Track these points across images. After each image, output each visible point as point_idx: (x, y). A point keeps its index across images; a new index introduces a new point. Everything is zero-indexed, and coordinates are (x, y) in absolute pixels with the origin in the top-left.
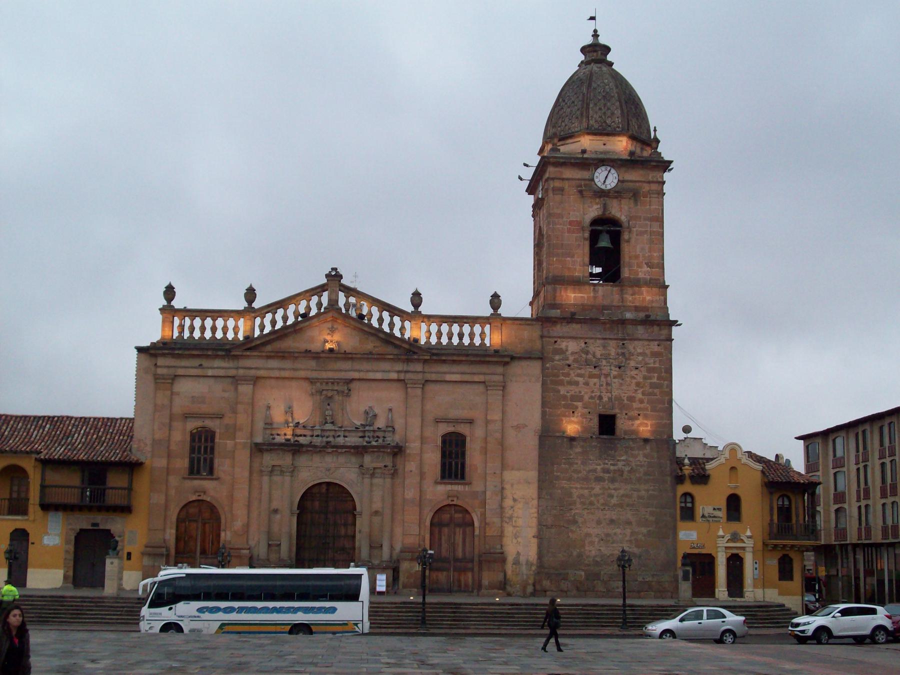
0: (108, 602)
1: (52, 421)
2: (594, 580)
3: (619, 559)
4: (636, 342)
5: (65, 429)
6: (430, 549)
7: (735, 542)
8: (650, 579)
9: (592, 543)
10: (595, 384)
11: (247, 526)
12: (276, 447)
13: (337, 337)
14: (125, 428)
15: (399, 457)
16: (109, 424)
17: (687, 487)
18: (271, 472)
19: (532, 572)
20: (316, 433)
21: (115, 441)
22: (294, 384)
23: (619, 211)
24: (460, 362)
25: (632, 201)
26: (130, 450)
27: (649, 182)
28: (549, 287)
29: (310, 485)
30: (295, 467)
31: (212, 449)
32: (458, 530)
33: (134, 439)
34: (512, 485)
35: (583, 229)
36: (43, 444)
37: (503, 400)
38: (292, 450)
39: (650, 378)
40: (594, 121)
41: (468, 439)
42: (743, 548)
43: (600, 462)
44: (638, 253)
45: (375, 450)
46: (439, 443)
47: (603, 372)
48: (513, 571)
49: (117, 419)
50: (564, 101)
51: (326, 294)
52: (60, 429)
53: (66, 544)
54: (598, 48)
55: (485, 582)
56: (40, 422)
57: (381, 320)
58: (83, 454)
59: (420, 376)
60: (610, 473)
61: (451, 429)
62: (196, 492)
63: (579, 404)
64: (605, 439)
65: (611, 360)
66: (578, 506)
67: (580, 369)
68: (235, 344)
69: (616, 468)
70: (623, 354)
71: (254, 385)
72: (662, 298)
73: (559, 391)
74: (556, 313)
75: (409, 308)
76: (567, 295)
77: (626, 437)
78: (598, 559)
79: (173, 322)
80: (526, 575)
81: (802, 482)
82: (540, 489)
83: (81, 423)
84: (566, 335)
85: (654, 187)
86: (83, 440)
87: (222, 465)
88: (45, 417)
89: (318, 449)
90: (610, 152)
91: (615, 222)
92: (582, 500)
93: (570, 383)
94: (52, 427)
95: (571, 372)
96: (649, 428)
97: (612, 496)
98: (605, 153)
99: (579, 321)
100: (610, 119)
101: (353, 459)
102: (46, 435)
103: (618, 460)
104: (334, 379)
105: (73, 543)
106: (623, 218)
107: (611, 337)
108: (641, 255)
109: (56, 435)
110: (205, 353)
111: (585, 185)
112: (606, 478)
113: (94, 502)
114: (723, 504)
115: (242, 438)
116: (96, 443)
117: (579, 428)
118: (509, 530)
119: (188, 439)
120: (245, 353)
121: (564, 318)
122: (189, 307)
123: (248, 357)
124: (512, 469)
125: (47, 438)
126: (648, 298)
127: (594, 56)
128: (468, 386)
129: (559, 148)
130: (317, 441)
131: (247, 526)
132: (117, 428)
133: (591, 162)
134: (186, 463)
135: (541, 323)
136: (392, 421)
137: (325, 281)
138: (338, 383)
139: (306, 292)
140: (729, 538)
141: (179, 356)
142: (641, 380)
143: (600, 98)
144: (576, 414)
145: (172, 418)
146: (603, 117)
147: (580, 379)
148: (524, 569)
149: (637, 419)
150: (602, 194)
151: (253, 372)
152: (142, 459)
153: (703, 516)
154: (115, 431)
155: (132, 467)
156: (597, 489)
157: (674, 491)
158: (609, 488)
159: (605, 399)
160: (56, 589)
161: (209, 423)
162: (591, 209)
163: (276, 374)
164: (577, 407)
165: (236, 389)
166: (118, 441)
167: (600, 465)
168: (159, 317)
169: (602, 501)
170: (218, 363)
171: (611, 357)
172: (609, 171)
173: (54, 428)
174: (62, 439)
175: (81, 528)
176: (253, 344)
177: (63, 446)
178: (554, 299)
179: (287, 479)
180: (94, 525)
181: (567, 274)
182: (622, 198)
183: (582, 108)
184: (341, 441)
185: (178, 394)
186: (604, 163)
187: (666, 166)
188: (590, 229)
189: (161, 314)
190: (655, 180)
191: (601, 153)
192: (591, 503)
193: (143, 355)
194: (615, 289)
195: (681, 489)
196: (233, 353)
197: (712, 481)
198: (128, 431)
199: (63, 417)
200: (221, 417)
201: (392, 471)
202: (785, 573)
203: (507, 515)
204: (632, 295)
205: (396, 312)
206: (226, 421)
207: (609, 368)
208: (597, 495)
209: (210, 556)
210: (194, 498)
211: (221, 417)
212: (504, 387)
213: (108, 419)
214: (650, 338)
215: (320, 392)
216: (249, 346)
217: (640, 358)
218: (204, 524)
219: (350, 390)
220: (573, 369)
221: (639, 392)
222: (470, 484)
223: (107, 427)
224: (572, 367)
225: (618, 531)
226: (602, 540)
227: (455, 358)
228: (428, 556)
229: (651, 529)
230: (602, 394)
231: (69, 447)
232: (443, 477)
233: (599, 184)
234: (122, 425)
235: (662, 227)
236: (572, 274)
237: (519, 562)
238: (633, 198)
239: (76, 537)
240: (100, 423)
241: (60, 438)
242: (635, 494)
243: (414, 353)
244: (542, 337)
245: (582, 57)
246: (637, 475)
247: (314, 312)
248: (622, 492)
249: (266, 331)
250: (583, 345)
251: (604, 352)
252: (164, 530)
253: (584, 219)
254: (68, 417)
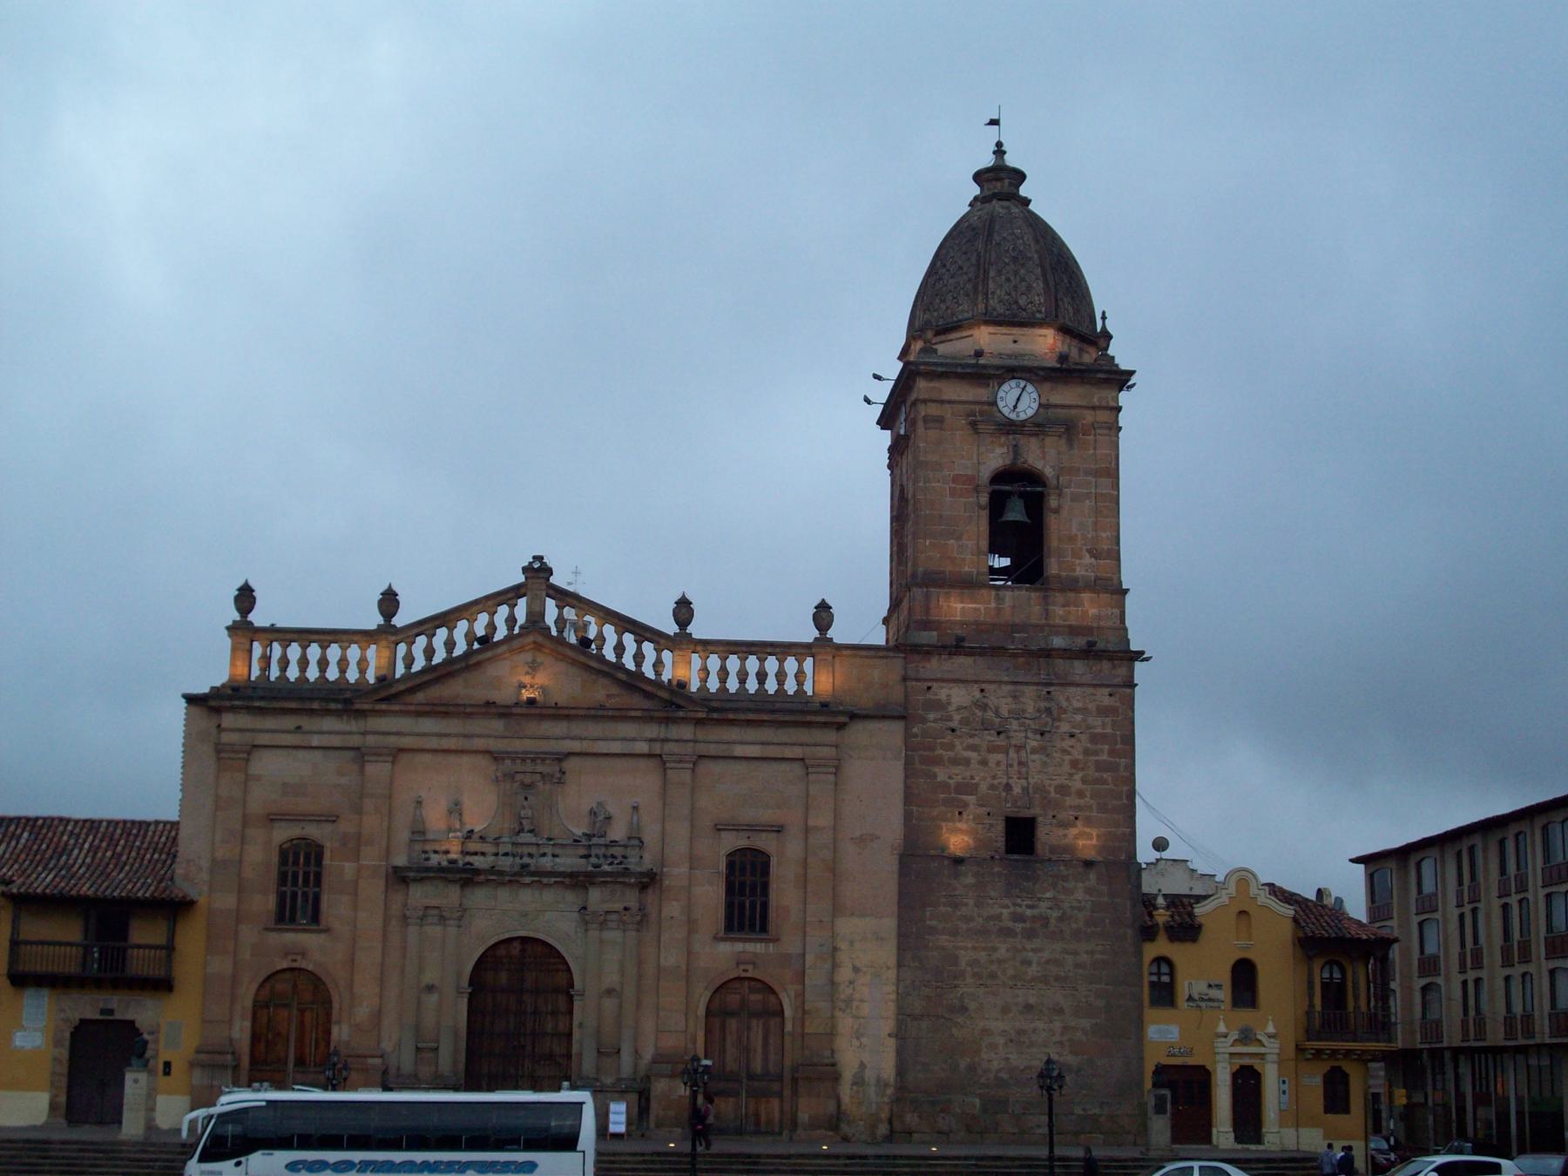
0: (129, 1152)
1: (33, 826)
2: (997, 1113)
3: (1041, 1075)
4: (1072, 690)
5: (55, 839)
6: (706, 1058)
7: (1246, 1045)
8: (1097, 1111)
9: (993, 1047)
10: (998, 764)
11: (378, 1015)
12: (431, 875)
13: (541, 678)
14: (163, 839)
15: (650, 891)
16: (135, 831)
17: (1161, 946)
18: (422, 920)
19: (886, 1099)
20: (502, 850)
21: (146, 862)
22: (466, 760)
23: (1041, 457)
24: (760, 723)
25: (1063, 441)
26: (172, 879)
27: (1094, 408)
28: (918, 592)
29: (492, 942)
30: (465, 910)
31: (318, 877)
32: (754, 1022)
33: (178, 860)
34: (852, 943)
35: (977, 489)
36: (16, 866)
37: (836, 790)
38: (461, 879)
39: (1096, 753)
40: (996, 301)
41: (774, 861)
42: (1262, 1056)
43: (1006, 901)
44: (1074, 531)
45: (609, 879)
46: (723, 866)
47: (1013, 742)
48: (852, 1097)
49: (148, 824)
50: (945, 266)
51: (522, 603)
52: (47, 841)
53: (55, 1047)
54: (1003, 175)
55: (803, 1117)
56: (12, 828)
57: (620, 649)
58: (87, 885)
59: (689, 748)
60: (1024, 921)
61: (742, 842)
62: (286, 954)
63: (971, 799)
64: (1016, 860)
65: (1027, 721)
66: (969, 980)
67: (972, 736)
68: (361, 690)
69: (1035, 912)
70: (1048, 711)
71: (393, 763)
72: (1117, 611)
73: (935, 776)
74: (930, 637)
75: (671, 628)
76: (949, 606)
77: (1054, 858)
78: (1005, 1076)
79: (250, 651)
80: (877, 1103)
81: (1365, 937)
82: (902, 948)
83: (85, 830)
84: (947, 676)
85: (1103, 416)
86: (88, 860)
87: (334, 906)
88: (19, 819)
89: (507, 878)
90: (1024, 355)
91: (1032, 478)
92: (975, 970)
93: (955, 761)
94: (33, 837)
95: (957, 742)
96: (1094, 842)
97: (1027, 963)
98: (1016, 356)
99: (971, 652)
100: (1024, 297)
101: (570, 896)
102: (22, 851)
103: (1040, 899)
104: (536, 753)
105: (67, 1043)
106: (1049, 472)
107: (1027, 679)
108: (1080, 537)
109: (41, 852)
110: (307, 705)
111: (982, 413)
112: (1018, 930)
113: (106, 971)
114: (1225, 978)
115: (371, 857)
116: (111, 866)
117: (971, 841)
118: (845, 1024)
119: (275, 859)
120: (378, 707)
121: (944, 647)
122: (280, 624)
123: (383, 713)
124: (852, 914)
125: (23, 856)
126: (1093, 611)
127: (998, 187)
128: (775, 766)
129: (935, 347)
130: (505, 863)
131: (378, 1016)
132: (148, 839)
133: (992, 372)
134: (271, 902)
135: (903, 655)
136: (639, 828)
137: (521, 579)
138: (543, 760)
139: (488, 598)
140: (1236, 1037)
141: (261, 711)
142: (1081, 757)
143: (1007, 260)
144: (965, 816)
145: (246, 821)
146: (1013, 294)
147: (973, 755)
148: (872, 1091)
149: (1073, 825)
150: (1011, 428)
151: (392, 741)
152: (193, 894)
153: (1190, 999)
154: (145, 845)
155: (175, 908)
156: (1003, 950)
157: (1139, 954)
158: (1024, 949)
159: (1017, 790)
160: (34, 1128)
161: (313, 831)
162: (991, 455)
163: (434, 743)
164: (966, 805)
165: (362, 771)
166: (150, 861)
167: (1007, 907)
168: (227, 642)
169: (1011, 972)
170: (329, 723)
171: (1028, 716)
172: (1023, 389)
173: (36, 839)
174: (51, 858)
175: (83, 1017)
176: (393, 691)
177: (52, 869)
178: (927, 610)
179: (452, 931)
180: (103, 1012)
181: (948, 568)
182: (1045, 434)
183: (976, 277)
184: (547, 863)
185: (258, 778)
186: (1015, 374)
187: (1122, 379)
188: (990, 489)
189: (230, 636)
190: (1104, 404)
191: (1010, 356)
192: (993, 976)
193: (195, 710)
194: (1033, 594)
195: (1151, 951)
196: (357, 706)
197: (1205, 935)
198: (168, 844)
199: (53, 819)
200: (333, 819)
201: (639, 918)
202: (1336, 1100)
203: (842, 997)
204: (1063, 606)
205: (648, 635)
206: (347, 826)
207: (1023, 735)
208: (1000, 962)
209: (312, 1069)
210: (285, 965)
211: (333, 819)
212: (837, 768)
213: (133, 822)
214: (1095, 682)
215: (511, 776)
216: (383, 694)
217: (1079, 718)
218: (302, 1012)
219: (564, 773)
220: (960, 737)
221: (1076, 777)
222: (778, 940)
223: (132, 838)
224: (958, 732)
225: (1040, 1025)
226: (1011, 1041)
227: (751, 716)
228: (701, 1069)
229: (1098, 1021)
230: (1010, 781)
231: (63, 872)
232: (729, 927)
233: (1006, 411)
234: (158, 833)
235: (1116, 485)
236: (957, 570)
237: (863, 1079)
238: (1065, 436)
239: (72, 1034)
240: (119, 831)
241: (47, 856)
242: (1070, 959)
243: (679, 707)
244: (905, 679)
245: (976, 190)
246: (1074, 926)
247: (501, 633)
248: (1046, 955)
249: (416, 667)
250: (978, 695)
251: (1014, 706)
252: (230, 1022)
253: (979, 472)
254: (61, 819)
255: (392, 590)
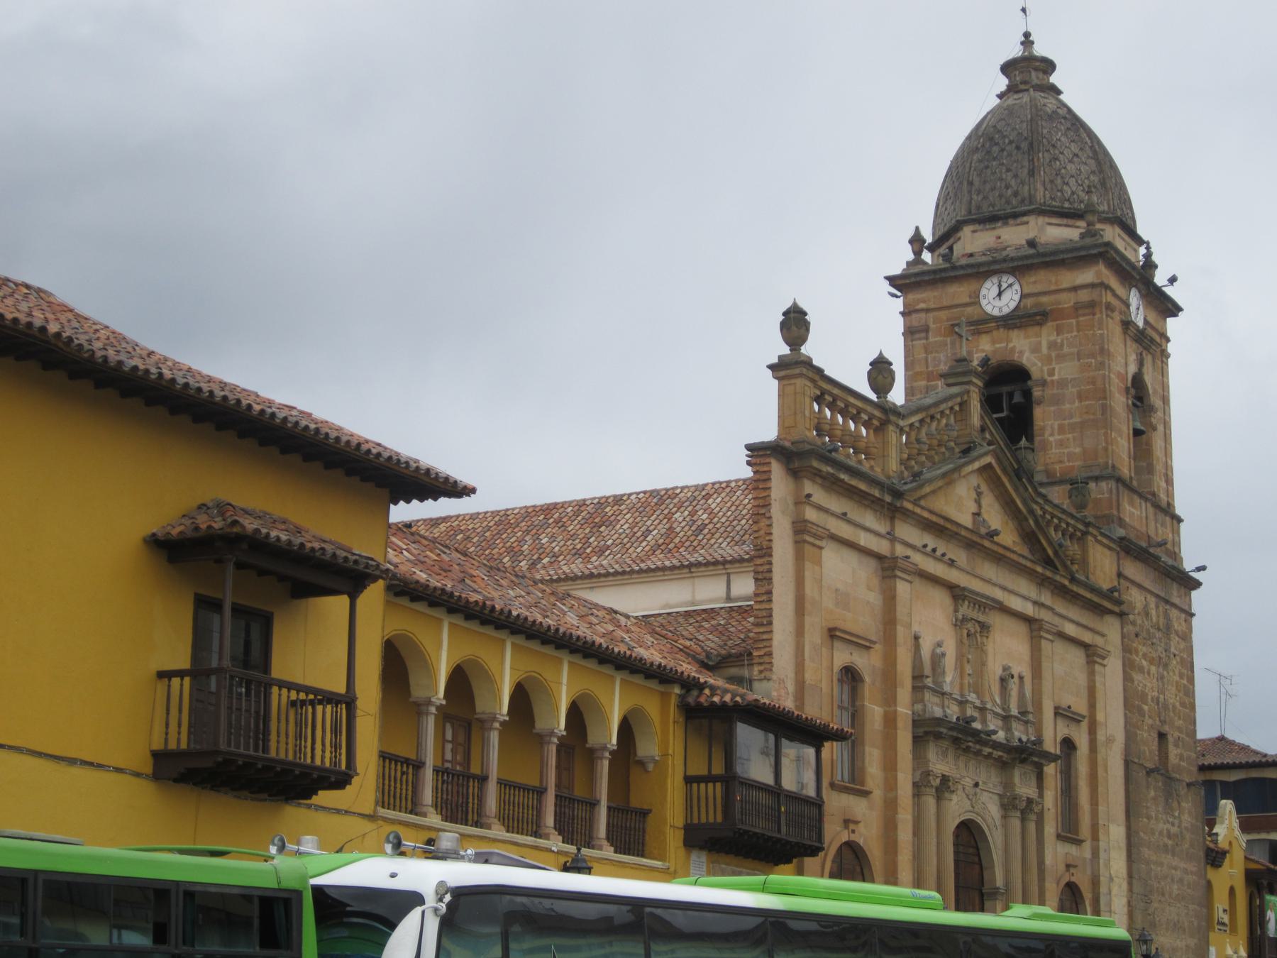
122: (827, 372)
170: (869, 519)
255: (884, 358)
